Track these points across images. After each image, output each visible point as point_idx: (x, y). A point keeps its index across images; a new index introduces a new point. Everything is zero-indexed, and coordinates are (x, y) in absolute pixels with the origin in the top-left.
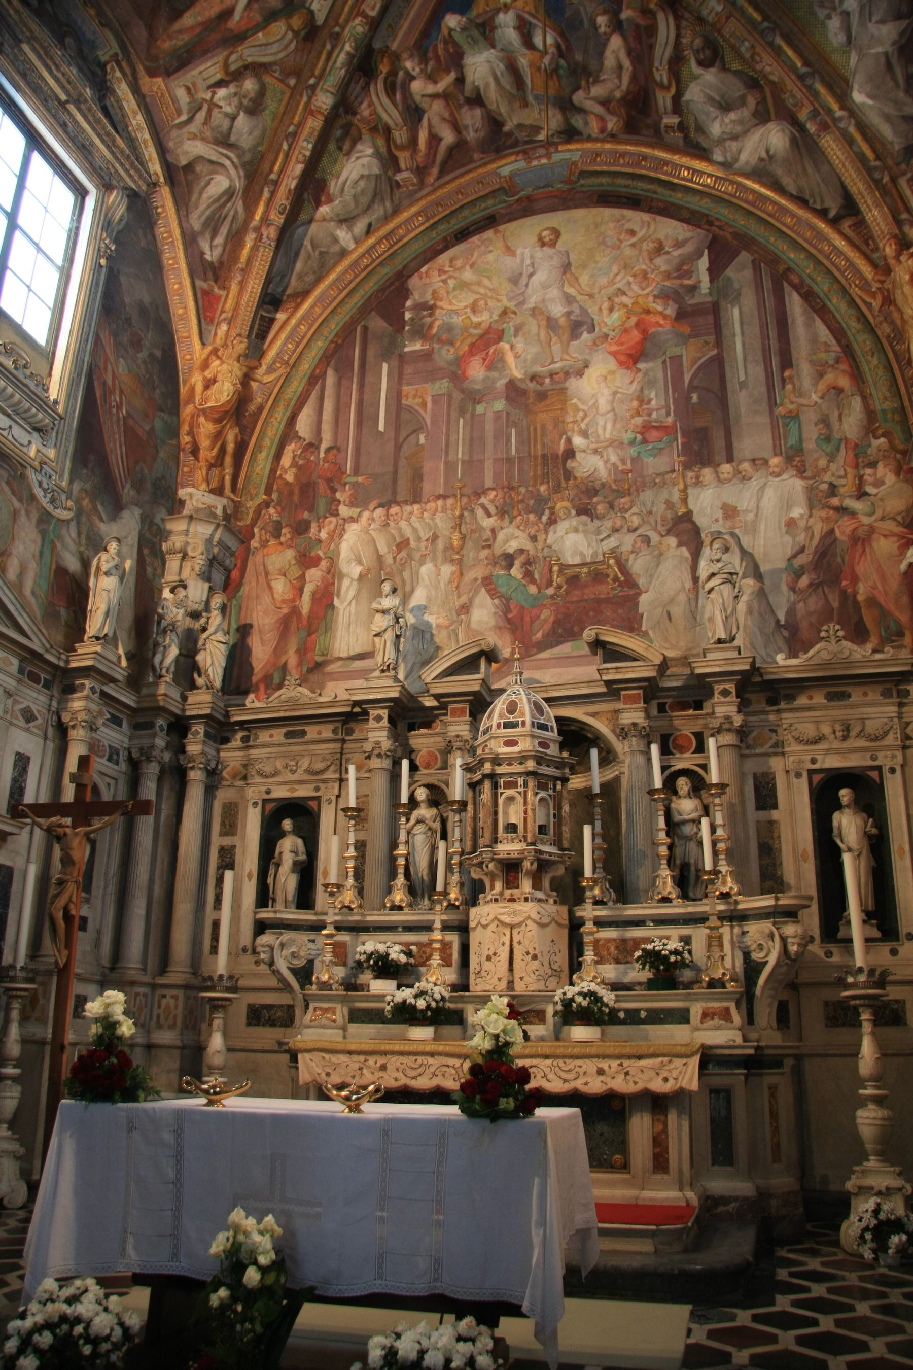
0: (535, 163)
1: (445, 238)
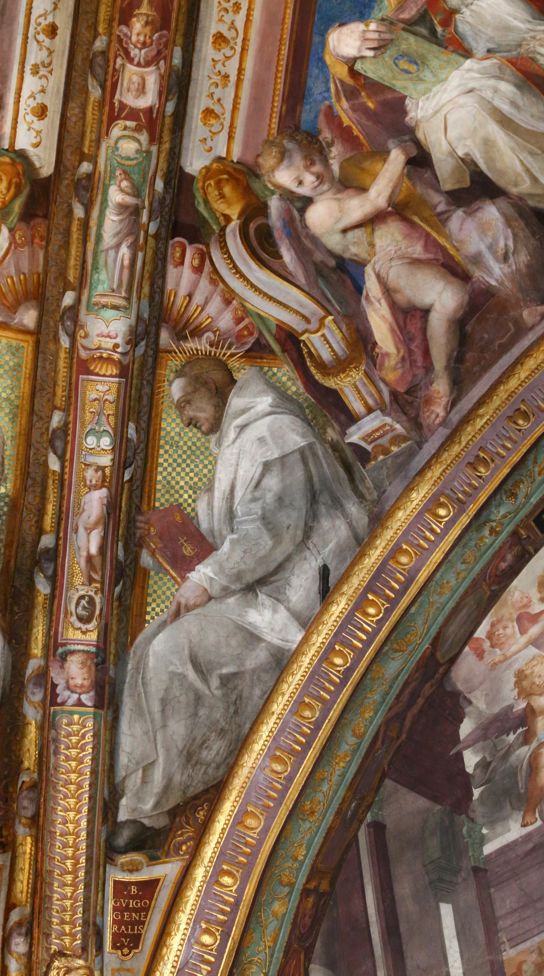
1: (515, 534)
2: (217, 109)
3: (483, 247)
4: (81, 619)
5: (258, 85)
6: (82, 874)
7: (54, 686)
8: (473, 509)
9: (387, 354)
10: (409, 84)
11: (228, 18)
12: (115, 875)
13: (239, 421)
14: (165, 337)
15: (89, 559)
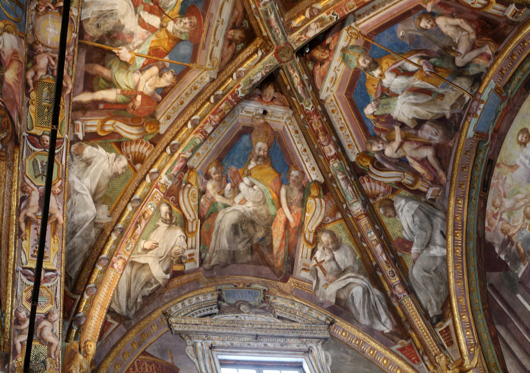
0: (479, 112)
2: (350, 143)
3: (430, 135)
4: (392, 277)
5: (356, 133)
6: (429, 334)
7: (396, 295)
8: (467, 197)
9: (424, 173)
10: (389, 110)
11: (340, 122)
12: (438, 330)
13: (400, 210)
14: (371, 201)
15: (386, 262)
